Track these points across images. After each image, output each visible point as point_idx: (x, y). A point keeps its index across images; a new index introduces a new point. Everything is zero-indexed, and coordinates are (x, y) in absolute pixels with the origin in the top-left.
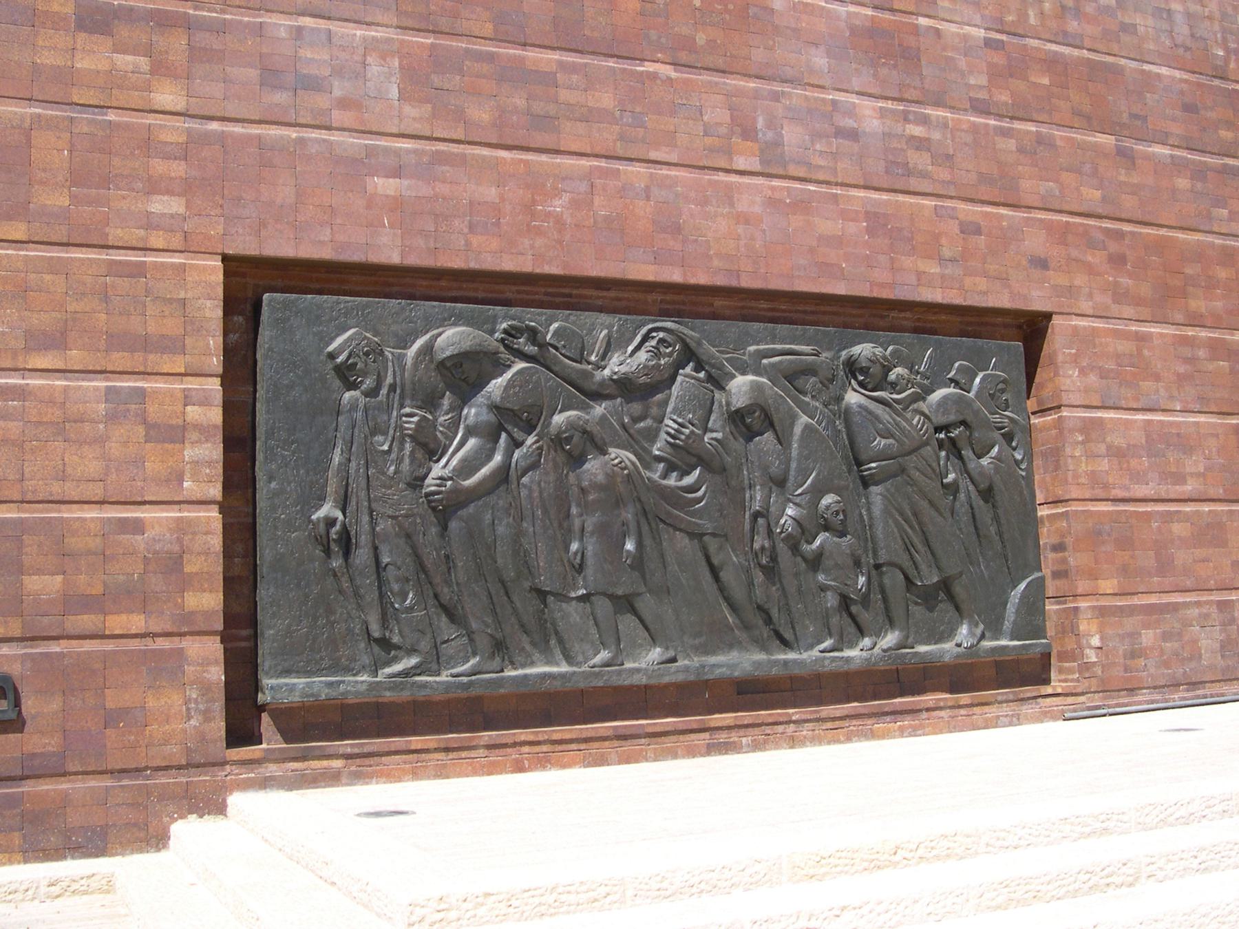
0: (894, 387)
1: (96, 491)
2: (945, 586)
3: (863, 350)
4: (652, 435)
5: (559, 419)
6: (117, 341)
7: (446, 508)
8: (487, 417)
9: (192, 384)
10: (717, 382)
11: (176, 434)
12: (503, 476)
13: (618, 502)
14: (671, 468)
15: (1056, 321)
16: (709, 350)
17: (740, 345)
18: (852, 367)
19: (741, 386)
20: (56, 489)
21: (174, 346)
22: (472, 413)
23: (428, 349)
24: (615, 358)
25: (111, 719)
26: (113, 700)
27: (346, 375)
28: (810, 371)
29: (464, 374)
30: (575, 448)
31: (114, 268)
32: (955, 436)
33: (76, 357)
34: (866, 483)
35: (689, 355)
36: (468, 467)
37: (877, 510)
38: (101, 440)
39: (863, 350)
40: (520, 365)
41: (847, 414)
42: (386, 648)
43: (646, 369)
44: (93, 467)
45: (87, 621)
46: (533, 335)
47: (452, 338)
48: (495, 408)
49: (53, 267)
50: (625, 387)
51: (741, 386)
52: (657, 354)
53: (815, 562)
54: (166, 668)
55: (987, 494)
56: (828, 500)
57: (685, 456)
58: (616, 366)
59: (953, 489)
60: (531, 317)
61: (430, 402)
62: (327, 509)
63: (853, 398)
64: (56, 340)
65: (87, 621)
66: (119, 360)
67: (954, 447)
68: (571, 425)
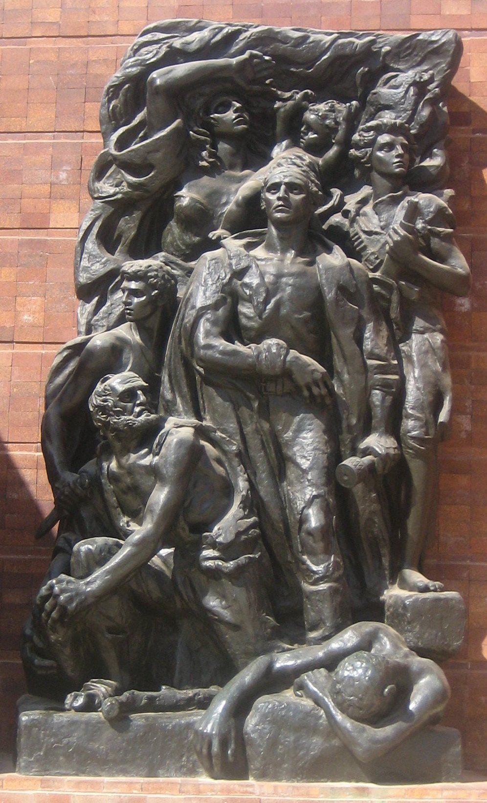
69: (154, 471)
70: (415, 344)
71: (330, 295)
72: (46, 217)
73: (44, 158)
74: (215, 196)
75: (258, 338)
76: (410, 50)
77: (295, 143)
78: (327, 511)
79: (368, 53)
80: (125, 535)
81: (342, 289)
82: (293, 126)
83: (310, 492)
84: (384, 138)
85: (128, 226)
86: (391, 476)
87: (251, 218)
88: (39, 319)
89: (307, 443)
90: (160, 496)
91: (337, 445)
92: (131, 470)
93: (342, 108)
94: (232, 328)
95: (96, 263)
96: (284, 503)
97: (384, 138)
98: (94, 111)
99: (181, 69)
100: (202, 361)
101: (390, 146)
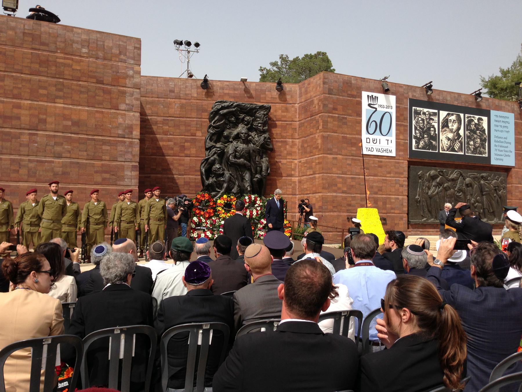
0: (488, 180)
1: (394, 194)
2: (493, 212)
3: (484, 174)
4: (455, 187)
5: (445, 185)
6: (396, 173)
7: (431, 197)
8: (436, 184)
9: (404, 179)
10: (464, 179)
11: (402, 186)
12: (437, 193)
13: (452, 197)
14: (458, 192)
15: (513, 169)
16: (463, 174)
17: (467, 174)
18: (482, 177)
19: (468, 180)
20: (390, 193)
21: (402, 174)
22: (434, 183)
23: (429, 174)
24: (452, 176)
25: (396, 224)
26: (396, 222)
27: (420, 178)
28: (477, 177)
29: (434, 178)
30: (446, 189)
31: (396, 162)
32: (497, 189)
33: (392, 175)
34: (483, 195)
35: (461, 175)
36: (433, 192)
37: (485, 200)
38: (394, 187)
39: (484, 174)
40: (441, 177)
41: (481, 185)
42: (423, 217)
43: (456, 177)
44: (394, 190)
45: (392, 211)
46: (442, 172)
47: (432, 172)
48: (437, 183)
49: (389, 162)
50: (453, 180)
51: (468, 180)
52: (457, 175)
53: (476, 207)
54: (401, 218)
55: (500, 198)
56: (478, 198)
57: (460, 190)
58: (452, 177)
59: (495, 197)
60: (441, 169)
61: (429, 182)
62: (417, 197)
63: (482, 182)
64: (389, 173)
65: (392, 211)
66: (397, 175)
67: (496, 190)
68: (447, 186)
69: (223, 181)
70: (264, 159)
71: (251, 151)
72: (195, 134)
73: (195, 123)
74: (230, 133)
75: (239, 158)
76: (262, 108)
77: (243, 124)
78: (250, 187)
79: (255, 108)
80: (219, 192)
81: (253, 151)
82: (243, 121)
83: (248, 184)
84: (260, 125)
85: (215, 138)
86: (260, 181)
87: (237, 137)
88: (195, 152)
89: (247, 176)
90: (225, 185)
91: (252, 176)
92: (219, 181)
93: (252, 119)
94: (235, 157)
95: (210, 144)
96: (244, 186)
97: (260, 125)
98: (206, 115)
99: (225, 111)
100: (230, 162)
101: (260, 126)
